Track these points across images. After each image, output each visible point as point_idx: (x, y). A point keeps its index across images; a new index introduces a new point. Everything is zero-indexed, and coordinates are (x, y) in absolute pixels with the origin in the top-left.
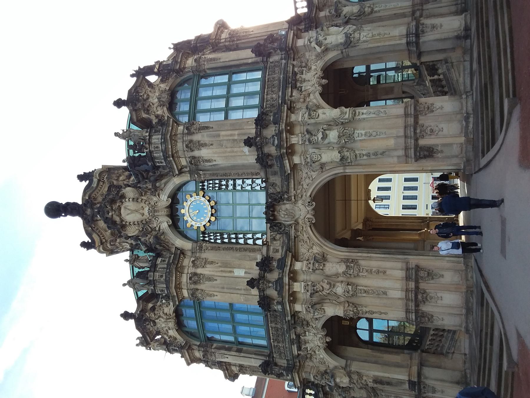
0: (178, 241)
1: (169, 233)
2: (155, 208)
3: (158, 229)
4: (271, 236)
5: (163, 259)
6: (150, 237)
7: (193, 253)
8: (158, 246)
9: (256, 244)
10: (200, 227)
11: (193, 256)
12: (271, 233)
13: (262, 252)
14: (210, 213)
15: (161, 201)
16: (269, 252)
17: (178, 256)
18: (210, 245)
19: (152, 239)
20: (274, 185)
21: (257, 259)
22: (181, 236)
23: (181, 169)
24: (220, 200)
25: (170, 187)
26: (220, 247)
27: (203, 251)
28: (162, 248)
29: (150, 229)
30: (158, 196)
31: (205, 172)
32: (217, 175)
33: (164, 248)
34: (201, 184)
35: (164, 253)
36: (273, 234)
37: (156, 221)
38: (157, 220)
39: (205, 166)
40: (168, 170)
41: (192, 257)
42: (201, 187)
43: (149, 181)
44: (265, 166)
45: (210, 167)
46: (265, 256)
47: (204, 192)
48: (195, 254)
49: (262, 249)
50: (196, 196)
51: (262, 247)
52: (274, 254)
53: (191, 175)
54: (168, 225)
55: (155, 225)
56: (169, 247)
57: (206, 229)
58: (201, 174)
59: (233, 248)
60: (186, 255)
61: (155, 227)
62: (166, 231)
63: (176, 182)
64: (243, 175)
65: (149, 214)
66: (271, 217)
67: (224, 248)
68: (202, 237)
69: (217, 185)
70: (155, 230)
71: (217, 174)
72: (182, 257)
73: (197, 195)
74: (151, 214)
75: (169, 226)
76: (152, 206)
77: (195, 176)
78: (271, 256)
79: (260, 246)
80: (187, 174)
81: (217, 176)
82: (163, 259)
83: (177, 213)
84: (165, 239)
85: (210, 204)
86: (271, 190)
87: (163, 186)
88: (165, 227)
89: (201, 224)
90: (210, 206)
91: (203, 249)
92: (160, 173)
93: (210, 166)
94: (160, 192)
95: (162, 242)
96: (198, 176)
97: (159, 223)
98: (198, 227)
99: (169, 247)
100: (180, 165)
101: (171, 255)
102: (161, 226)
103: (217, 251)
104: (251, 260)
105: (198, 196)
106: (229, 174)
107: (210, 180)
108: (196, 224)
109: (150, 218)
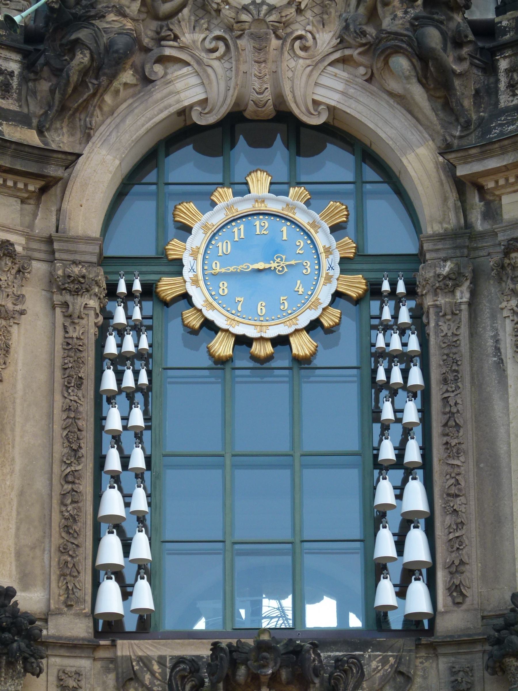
0: (109, 157)
1: (148, 114)
2: (275, 43)
3: (168, 52)
4: (145, 661)
5: (15, 83)
6: (124, 15)
7: (50, 241)
8: (86, 60)
9: (96, 585)
10: (180, 273)
11: (35, 245)
12: (161, 661)
13: (59, 613)
14: (251, 332)
15: (316, 74)
16: (62, 652)
17: (33, 168)
18: (93, 331)
19: (117, 25)
20: (399, 679)
21: (26, 587)
22: (126, 169)
23: (481, 189)
24: (312, 379)
25: (386, 122)
26: (79, 386)
27: (58, 298)
28: (74, 78)
29: (166, 8)
30: (337, 55)
31: (464, 315)
32: (450, 377)
33: (70, 90)
34: (401, 288)
35: (44, 86)
36: (153, 674)
37: (209, 45)
38: (213, 50)
39: (493, 317)
40: (474, 117)
41: (29, 238)
42: (386, 286)
43: (416, 18)
44: (498, 642)
45: (490, 342)
46: (44, 632)
47: (357, 301)
48: (42, 256)
49: (78, 615)
50: (336, 256)
51: (86, 616)
52: (52, 679)
53: (448, 244)
54: (191, 107)
55: (187, 38)
56: (76, 110)
57: (166, 304)
58: (453, 292)
59: (78, 459)
60: (38, 206)
61: (176, 38)
62: (157, 95)
63: (411, 157)
64: (448, 520)
65: (245, 8)
66: (248, 668)
67: (76, 411)
68: (129, 286)
69: (397, 377)
70: (165, 39)
71: (456, 380)
72: (31, 188)
73: (343, 261)
74: (244, 17)
75: (184, 112)
76: (286, 25)
77: (445, 260)
78: (44, 661)
79: (89, 598)
80: (452, 215)
81: (445, 381)
82: (15, 83)
83: (241, 138)
84: (117, 92)
85: (297, 331)
86: (374, 664)
87: (394, 85)
88: (178, 93)
89: (195, 282)
90: (283, 330)
91: (68, 298)
92: (460, 75)
93: (497, 341)
94: (362, 70)
95: (104, 80)
96: (447, 277)
97: (199, 62)
98: (179, 263)
99: (76, 110)
100: (503, 187)
101: (35, 122)
102: (185, 70)
103: (58, 374)
104: (18, 555)
105: (338, 269)
106: (454, 442)
107: (424, 342)
108: (194, 254)
109: (226, 11)
